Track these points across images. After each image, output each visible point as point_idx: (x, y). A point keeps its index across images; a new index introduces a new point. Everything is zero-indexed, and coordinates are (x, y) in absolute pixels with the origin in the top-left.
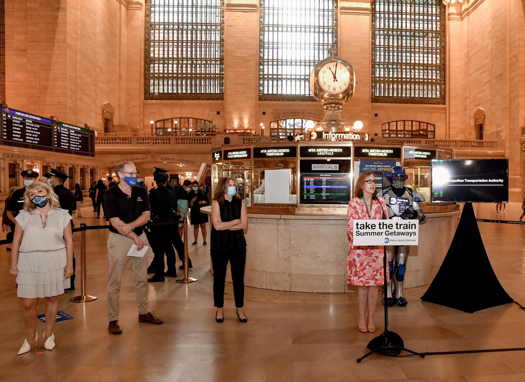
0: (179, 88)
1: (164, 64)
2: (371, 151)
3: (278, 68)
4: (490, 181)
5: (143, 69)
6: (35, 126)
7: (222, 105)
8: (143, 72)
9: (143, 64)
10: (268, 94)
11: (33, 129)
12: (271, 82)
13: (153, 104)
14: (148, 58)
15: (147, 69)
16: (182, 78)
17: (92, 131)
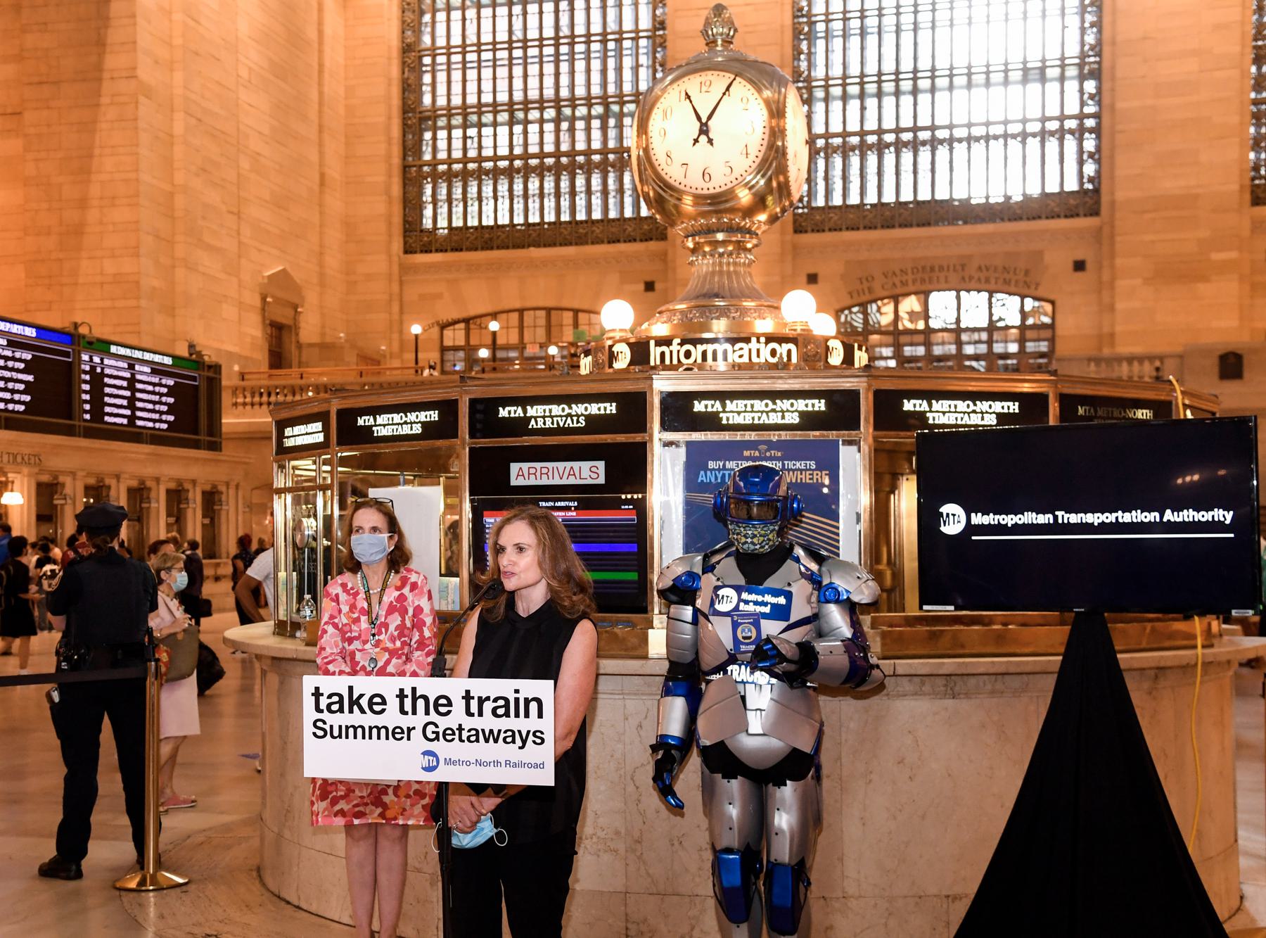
0: (611, 201)
1: (465, 126)
2: (936, 405)
3: (863, 108)
4: (1169, 515)
5: (396, 151)
6: (18, 355)
7: (663, 257)
8: (396, 160)
9: (396, 131)
10: (828, 208)
11: (10, 364)
12: (855, 160)
13: (430, 267)
14: (413, 110)
15: (411, 147)
16: (527, 172)
17: (210, 367)
